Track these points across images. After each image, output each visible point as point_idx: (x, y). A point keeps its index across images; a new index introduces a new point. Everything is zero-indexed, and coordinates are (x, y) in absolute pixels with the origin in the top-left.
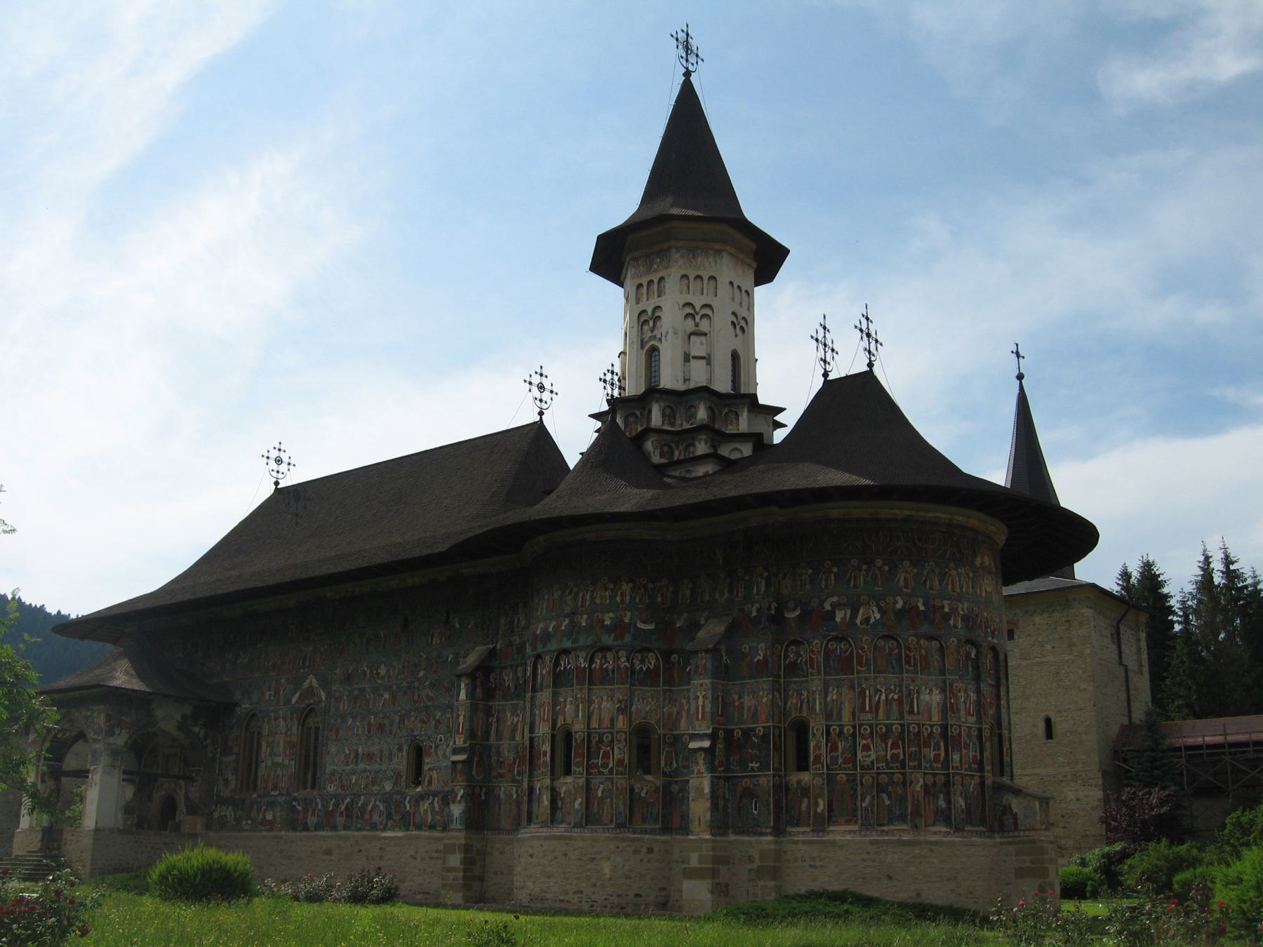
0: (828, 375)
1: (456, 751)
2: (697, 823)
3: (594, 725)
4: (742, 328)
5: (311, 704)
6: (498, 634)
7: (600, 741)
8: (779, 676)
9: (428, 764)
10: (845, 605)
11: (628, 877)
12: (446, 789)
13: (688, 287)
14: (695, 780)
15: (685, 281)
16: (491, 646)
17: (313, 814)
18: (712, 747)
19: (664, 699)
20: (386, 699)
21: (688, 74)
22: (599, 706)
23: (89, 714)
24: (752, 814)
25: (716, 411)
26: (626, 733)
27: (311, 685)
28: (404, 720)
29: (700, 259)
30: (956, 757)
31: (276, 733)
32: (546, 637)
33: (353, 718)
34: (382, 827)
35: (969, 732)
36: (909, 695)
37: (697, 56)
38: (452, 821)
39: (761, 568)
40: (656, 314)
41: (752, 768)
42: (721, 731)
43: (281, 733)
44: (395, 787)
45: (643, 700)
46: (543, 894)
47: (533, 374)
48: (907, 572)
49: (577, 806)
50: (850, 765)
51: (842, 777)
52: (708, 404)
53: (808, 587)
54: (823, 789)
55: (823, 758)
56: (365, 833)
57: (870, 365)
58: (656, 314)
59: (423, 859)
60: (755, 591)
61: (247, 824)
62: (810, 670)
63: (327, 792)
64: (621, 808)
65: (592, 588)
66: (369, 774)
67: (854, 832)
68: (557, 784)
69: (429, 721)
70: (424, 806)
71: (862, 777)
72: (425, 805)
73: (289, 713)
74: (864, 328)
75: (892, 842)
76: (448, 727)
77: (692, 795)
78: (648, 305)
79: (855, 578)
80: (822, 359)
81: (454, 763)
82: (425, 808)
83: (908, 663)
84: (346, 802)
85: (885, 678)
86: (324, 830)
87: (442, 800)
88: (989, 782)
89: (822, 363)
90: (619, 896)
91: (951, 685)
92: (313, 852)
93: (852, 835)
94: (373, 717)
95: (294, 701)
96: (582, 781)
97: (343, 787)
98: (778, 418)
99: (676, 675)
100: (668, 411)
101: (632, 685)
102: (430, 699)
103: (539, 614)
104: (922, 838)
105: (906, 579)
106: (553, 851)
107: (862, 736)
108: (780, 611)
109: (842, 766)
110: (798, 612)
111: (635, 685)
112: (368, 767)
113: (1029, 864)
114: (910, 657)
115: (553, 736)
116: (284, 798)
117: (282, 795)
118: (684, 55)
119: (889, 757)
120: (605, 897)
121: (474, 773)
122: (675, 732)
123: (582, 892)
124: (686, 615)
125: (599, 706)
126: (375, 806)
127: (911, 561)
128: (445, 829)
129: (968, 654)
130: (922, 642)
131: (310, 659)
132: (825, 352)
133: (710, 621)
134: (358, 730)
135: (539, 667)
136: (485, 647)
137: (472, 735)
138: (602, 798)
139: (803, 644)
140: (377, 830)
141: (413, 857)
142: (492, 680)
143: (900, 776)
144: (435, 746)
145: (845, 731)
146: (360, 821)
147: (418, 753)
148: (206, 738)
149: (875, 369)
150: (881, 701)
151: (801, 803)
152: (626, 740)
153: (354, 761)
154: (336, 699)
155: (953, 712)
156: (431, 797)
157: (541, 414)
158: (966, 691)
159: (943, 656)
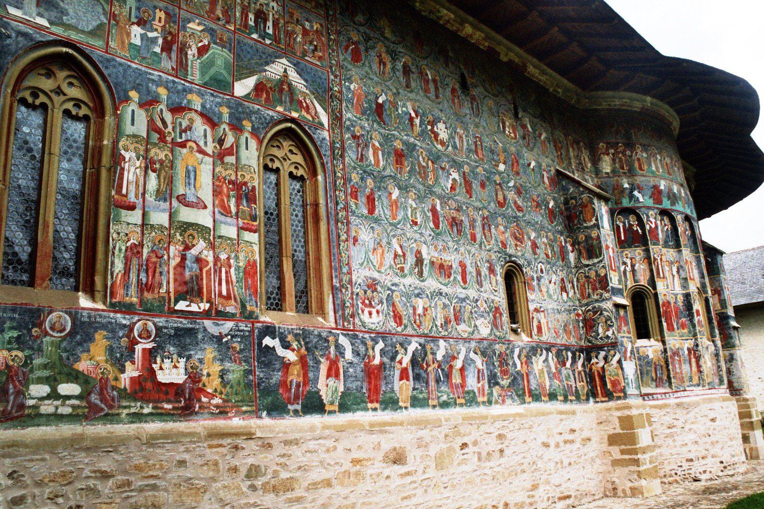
5: (293, 120)
6: (570, 164)
9: (532, 301)
12: (559, 341)
17: (333, 372)
20: (454, 180)
28: (489, 226)
31: (183, 145)
34: (485, 399)
43: (201, 151)
44: (495, 330)
59: (557, 445)
61: (54, 395)
63: (363, 324)
66: (447, 302)
69: (523, 237)
70: (537, 362)
72: (538, 363)
73: (225, 111)
76: (547, 256)
81: (617, 306)
82: (540, 367)
84: (411, 348)
86: (366, 409)
92: (355, 462)
94: (438, 202)
97: (398, 318)
102: (519, 209)
112: (445, 289)
116: (230, 325)
126: (468, 361)
131: (275, 24)
140: (478, 404)
144: (537, 277)
153: (416, 270)
154: (354, 137)
156: (544, 352)
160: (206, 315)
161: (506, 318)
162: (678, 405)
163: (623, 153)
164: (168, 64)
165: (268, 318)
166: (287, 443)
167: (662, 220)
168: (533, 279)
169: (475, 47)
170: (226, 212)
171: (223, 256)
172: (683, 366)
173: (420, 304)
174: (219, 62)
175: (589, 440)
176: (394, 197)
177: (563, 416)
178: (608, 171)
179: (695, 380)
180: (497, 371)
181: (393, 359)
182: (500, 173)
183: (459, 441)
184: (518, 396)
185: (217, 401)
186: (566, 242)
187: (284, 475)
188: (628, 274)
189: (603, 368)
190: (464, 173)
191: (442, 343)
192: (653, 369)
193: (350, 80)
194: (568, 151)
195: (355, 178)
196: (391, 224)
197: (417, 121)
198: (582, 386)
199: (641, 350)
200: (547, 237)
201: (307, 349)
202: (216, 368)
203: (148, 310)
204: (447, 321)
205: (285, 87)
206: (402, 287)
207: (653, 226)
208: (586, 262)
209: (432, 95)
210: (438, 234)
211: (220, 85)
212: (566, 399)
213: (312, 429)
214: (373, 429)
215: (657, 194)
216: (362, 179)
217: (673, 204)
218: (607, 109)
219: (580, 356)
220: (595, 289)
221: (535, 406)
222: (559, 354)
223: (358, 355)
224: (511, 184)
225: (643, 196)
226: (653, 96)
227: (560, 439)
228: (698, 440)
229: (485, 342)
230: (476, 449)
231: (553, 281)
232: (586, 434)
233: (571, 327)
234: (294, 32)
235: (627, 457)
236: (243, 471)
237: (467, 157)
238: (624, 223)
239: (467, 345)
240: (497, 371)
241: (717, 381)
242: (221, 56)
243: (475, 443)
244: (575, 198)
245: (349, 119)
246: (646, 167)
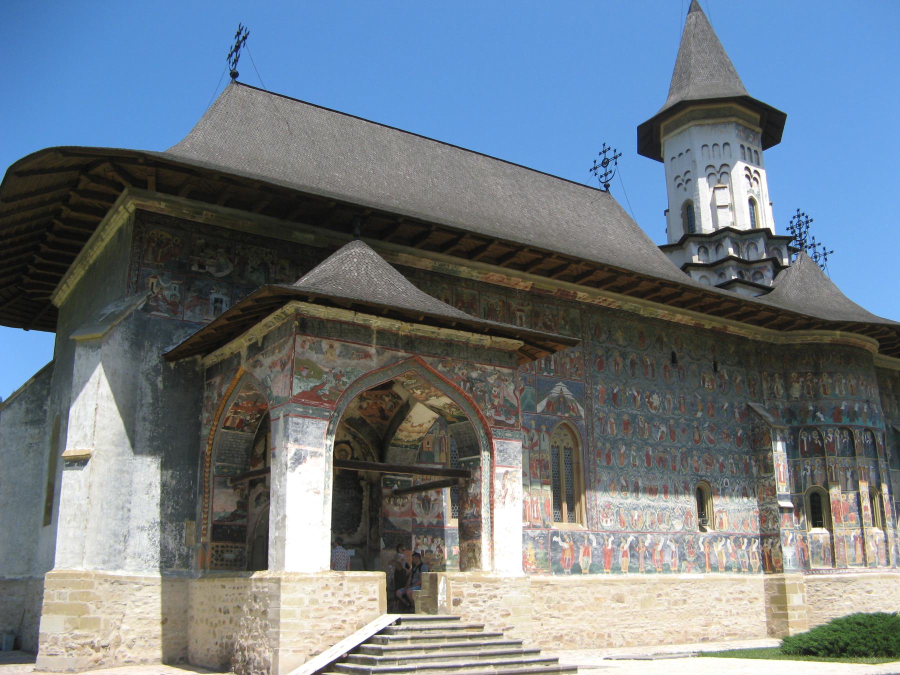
12: (737, 532)
17: (586, 553)
20: (663, 432)
23: (474, 375)
27: (561, 395)
33: (626, 445)
34: (676, 569)
56: (657, 574)
59: (728, 601)
66: (654, 511)
72: (718, 547)
73: (533, 422)
76: (732, 472)
82: (719, 549)
86: (603, 573)
92: (597, 599)
97: (622, 523)
102: (711, 441)
103: (837, 392)
112: (652, 504)
116: (538, 531)
117: (535, 527)
126: (665, 546)
140: (671, 572)
141: (719, 600)
146: (649, 562)
161: (695, 520)
162: (839, 580)
163: (812, 382)
165: (555, 526)
166: (565, 587)
167: (842, 433)
168: (718, 490)
169: (686, 326)
171: (535, 499)
172: (847, 549)
173: (636, 514)
174: (529, 396)
175: (757, 599)
176: (622, 451)
177: (734, 582)
178: (797, 396)
179: (860, 560)
181: (619, 545)
182: (697, 419)
183: (657, 592)
184: (700, 567)
185: (534, 567)
186: (750, 459)
187: (563, 602)
188: (807, 478)
189: (770, 550)
190: (670, 425)
191: (649, 536)
192: (822, 552)
193: (596, 384)
195: (599, 444)
196: (620, 468)
197: (639, 398)
198: (757, 562)
199: (813, 536)
200: (733, 459)
201: (574, 542)
202: (533, 552)
205: (561, 400)
206: (625, 505)
207: (831, 440)
208: (763, 475)
209: (650, 376)
210: (651, 469)
212: (739, 570)
213: (576, 581)
215: (837, 414)
216: (604, 444)
217: (852, 420)
218: (801, 344)
219: (755, 542)
220: (768, 495)
222: (736, 540)
223: (600, 544)
224: (706, 425)
225: (824, 416)
226: (841, 330)
227: (729, 596)
228: (853, 606)
229: (678, 534)
230: (667, 598)
231: (736, 489)
232: (753, 595)
233: (749, 521)
234: (565, 363)
235: (781, 612)
236: (545, 599)
237: (673, 414)
238: (808, 438)
239: (665, 536)
240: (686, 552)
241: (884, 561)
244: (758, 427)
245: (596, 409)
246: (830, 392)
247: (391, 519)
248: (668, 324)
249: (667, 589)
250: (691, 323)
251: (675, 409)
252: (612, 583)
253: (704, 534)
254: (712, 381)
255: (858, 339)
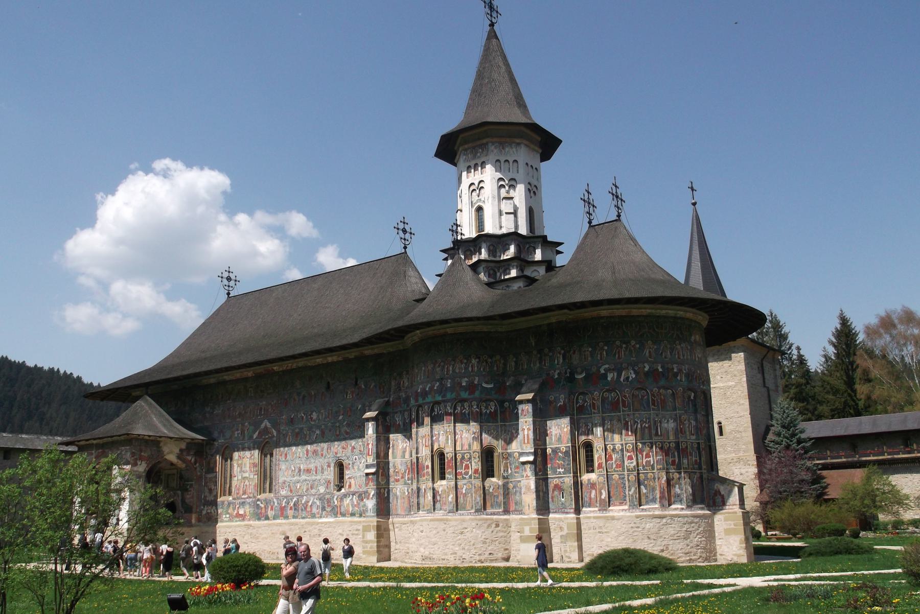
0: (591, 222)
1: (368, 467)
2: (528, 507)
3: (458, 448)
4: (534, 192)
5: (267, 438)
6: (390, 391)
7: (463, 458)
8: (574, 415)
10: (613, 370)
11: (484, 543)
12: (361, 490)
13: (500, 167)
14: (525, 481)
15: (498, 164)
16: (386, 399)
17: (272, 509)
18: (535, 459)
19: (501, 431)
21: (492, 25)
22: (461, 437)
24: (560, 501)
25: (521, 247)
26: (479, 453)
27: (266, 427)
29: (507, 149)
30: (685, 461)
32: (425, 394)
35: (692, 445)
36: (655, 424)
37: (497, 12)
38: (367, 511)
39: (559, 348)
40: (481, 185)
41: (560, 472)
42: (539, 450)
45: (488, 431)
46: (431, 556)
47: (399, 223)
48: (650, 348)
49: (450, 499)
50: (621, 469)
51: (616, 477)
52: (517, 243)
53: (589, 359)
54: (604, 484)
55: (604, 465)
56: (308, 520)
57: (619, 216)
58: (481, 185)
60: (556, 362)
62: (593, 410)
64: (478, 499)
65: (453, 363)
67: (626, 510)
68: (435, 485)
71: (628, 476)
72: (347, 501)
73: (252, 445)
74: (614, 193)
75: (650, 516)
77: (523, 490)
78: (475, 179)
79: (619, 352)
80: (587, 213)
81: (367, 474)
83: (653, 404)
84: (294, 500)
85: (639, 414)
87: (359, 497)
88: (705, 476)
89: (588, 215)
90: (480, 555)
91: (680, 417)
92: (272, 533)
93: (624, 512)
95: (255, 436)
96: (453, 483)
97: (291, 491)
98: (559, 248)
99: (507, 416)
100: (491, 248)
101: (481, 422)
104: (667, 513)
105: (650, 352)
106: (436, 528)
107: (628, 451)
108: (572, 374)
109: (616, 469)
110: (584, 375)
111: (483, 423)
112: (308, 478)
113: (733, 526)
114: (654, 401)
115: (432, 456)
116: (251, 499)
117: (250, 498)
118: (489, 12)
119: (644, 463)
120: (470, 556)
121: (380, 480)
122: (509, 451)
123: (456, 553)
124: (512, 378)
125: (461, 437)
126: (314, 503)
127: (652, 341)
128: (361, 516)
129: (690, 397)
130: (661, 391)
131: (264, 410)
132: (589, 208)
133: (528, 381)
134: (299, 454)
135: (420, 412)
136: (382, 400)
137: (378, 456)
138: (465, 495)
139: (587, 394)
140: (316, 518)
142: (388, 421)
143: (652, 474)
145: (617, 448)
147: (341, 467)
148: (195, 463)
149: (622, 218)
150: (638, 430)
151: (591, 492)
152: (479, 457)
155: (682, 433)
157: (405, 248)
158: (689, 421)
159: (674, 399)
160: (247, 498)
164: (241, 438)
169: (338, 362)
170: (251, 472)
180: (326, 505)
182: (338, 421)
187: (257, 535)
193: (283, 415)
194: (390, 383)
203: (238, 498)
204: (307, 489)
211: (251, 437)
214: (280, 525)
217: (424, 399)
221: (341, 519)
227: (348, 532)
240: (326, 505)
242: (252, 428)
243: (309, 531)
247: (186, 501)
248: (328, 365)
249: (310, 528)
250: (340, 359)
251: (325, 418)
252: (360, 522)
253: (338, 493)
254: (352, 393)
255: (434, 330)
